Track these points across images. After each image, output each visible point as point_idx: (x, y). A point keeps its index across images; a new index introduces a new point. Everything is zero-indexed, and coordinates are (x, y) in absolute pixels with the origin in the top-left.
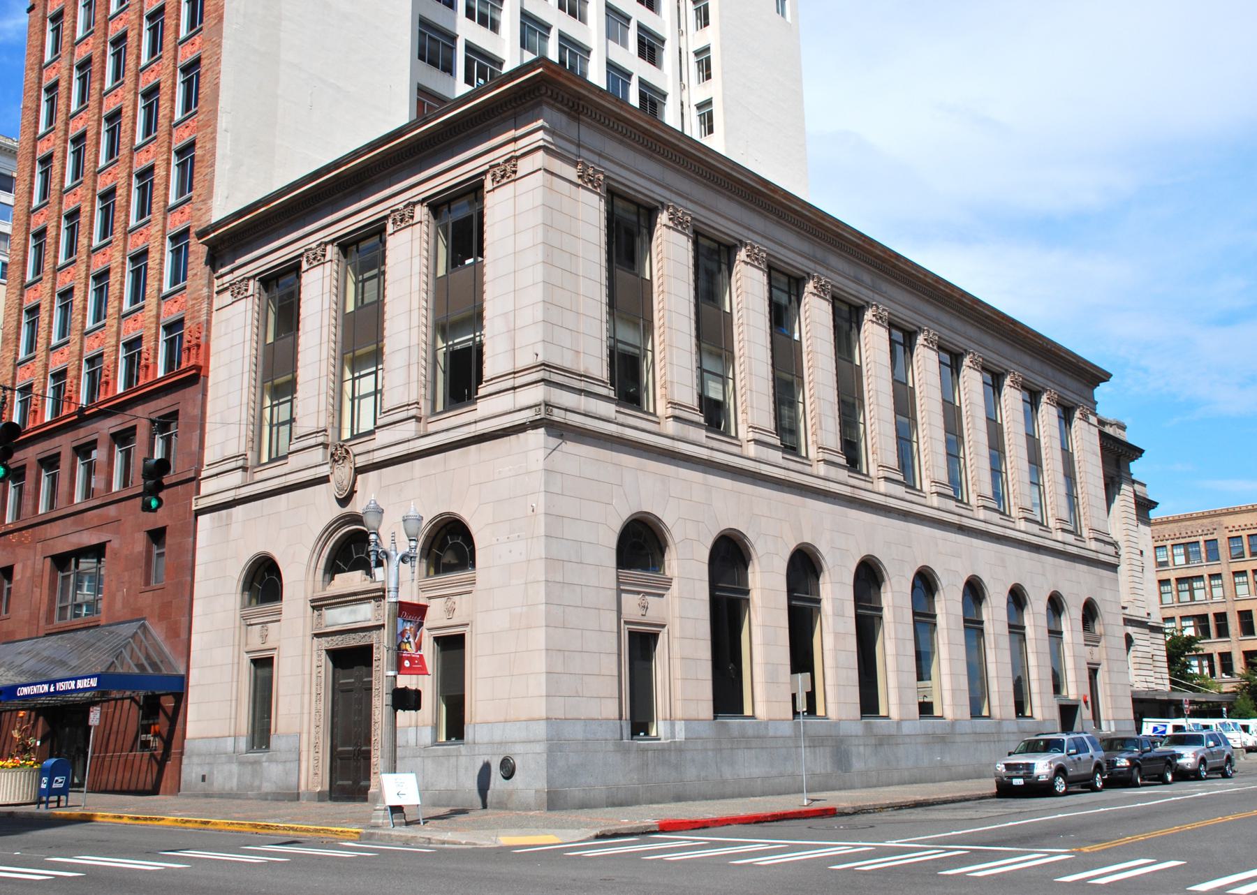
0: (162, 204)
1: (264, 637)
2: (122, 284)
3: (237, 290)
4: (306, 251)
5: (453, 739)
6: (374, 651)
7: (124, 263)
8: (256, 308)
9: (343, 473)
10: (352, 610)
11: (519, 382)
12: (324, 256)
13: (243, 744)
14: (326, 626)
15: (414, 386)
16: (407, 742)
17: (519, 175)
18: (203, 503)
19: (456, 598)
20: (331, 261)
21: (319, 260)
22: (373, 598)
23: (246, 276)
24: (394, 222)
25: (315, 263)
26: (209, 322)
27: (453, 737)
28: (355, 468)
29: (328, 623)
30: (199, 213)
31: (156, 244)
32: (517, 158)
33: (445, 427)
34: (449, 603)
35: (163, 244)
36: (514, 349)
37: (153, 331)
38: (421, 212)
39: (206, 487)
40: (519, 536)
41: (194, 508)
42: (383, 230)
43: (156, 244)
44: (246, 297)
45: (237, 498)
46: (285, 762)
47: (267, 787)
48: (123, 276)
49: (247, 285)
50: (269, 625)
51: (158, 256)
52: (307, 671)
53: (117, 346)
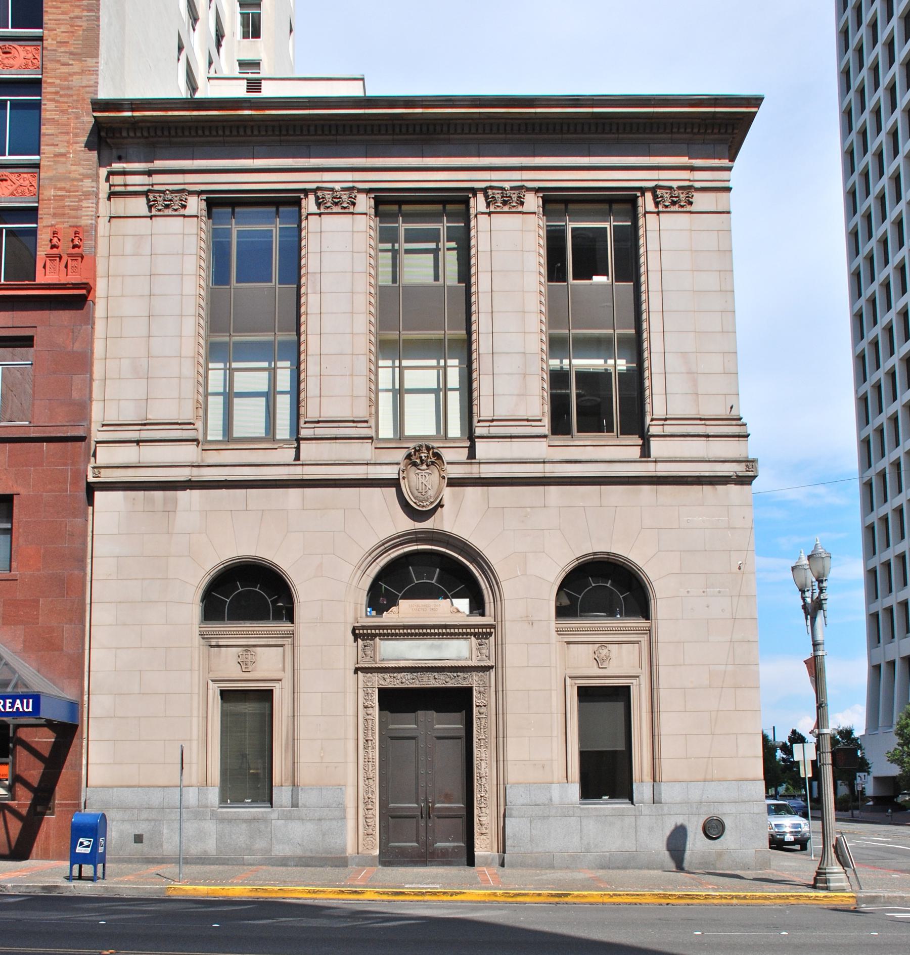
4: (318, 189)
5: (607, 798)
6: (475, 693)
10: (432, 644)
13: (213, 795)
14: (383, 660)
16: (551, 800)
18: (108, 476)
21: (345, 208)
22: (475, 634)
23: (187, 187)
27: (606, 795)
29: (385, 656)
33: (608, 458)
39: (104, 455)
40: (719, 592)
41: (91, 479)
45: (194, 479)
46: (320, 820)
47: (280, 850)
52: (351, 711)
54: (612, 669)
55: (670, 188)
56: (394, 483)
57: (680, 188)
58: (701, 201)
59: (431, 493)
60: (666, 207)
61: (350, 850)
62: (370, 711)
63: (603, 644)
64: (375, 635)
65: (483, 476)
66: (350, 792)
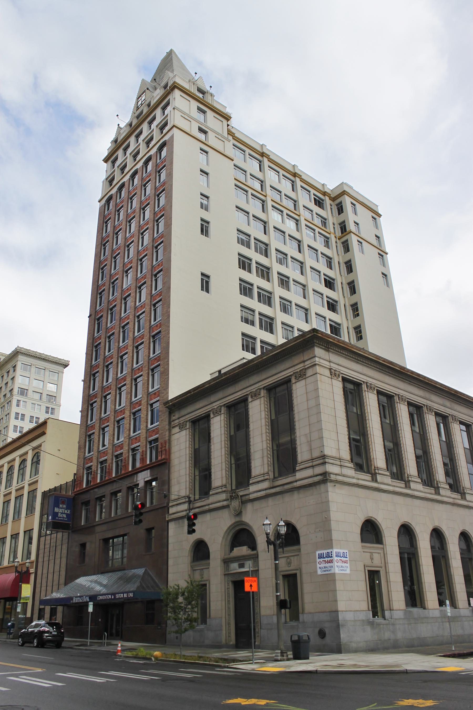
0: (146, 391)
1: (202, 575)
2: (130, 424)
3: (182, 427)
4: (212, 409)
7: (130, 416)
8: (190, 434)
9: (235, 504)
11: (315, 463)
12: (220, 411)
15: (266, 466)
17: (307, 376)
19: (292, 558)
20: (224, 413)
22: (253, 558)
24: (252, 397)
25: (217, 415)
26: (169, 440)
28: (241, 502)
30: (163, 395)
31: (145, 407)
32: (305, 369)
34: (289, 560)
35: (147, 408)
36: (311, 450)
37: (145, 444)
38: (263, 393)
39: (172, 510)
41: (167, 519)
42: (247, 399)
43: (145, 407)
44: (186, 429)
47: (207, 642)
48: (130, 421)
49: (186, 424)
50: (204, 570)
51: (145, 412)
52: (224, 590)
53: (129, 450)
54: (292, 568)
55: (297, 372)
56: (227, 507)
57: (300, 371)
58: (309, 372)
59: (237, 508)
60: (298, 379)
61: (224, 641)
62: (229, 590)
63: (288, 557)
64: (228, 562)
65: (250, 498)
66: (224, 620)
